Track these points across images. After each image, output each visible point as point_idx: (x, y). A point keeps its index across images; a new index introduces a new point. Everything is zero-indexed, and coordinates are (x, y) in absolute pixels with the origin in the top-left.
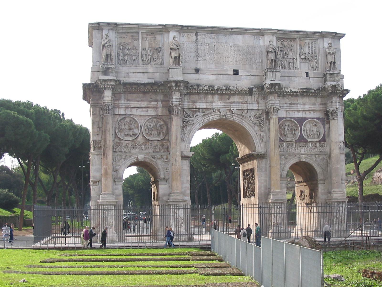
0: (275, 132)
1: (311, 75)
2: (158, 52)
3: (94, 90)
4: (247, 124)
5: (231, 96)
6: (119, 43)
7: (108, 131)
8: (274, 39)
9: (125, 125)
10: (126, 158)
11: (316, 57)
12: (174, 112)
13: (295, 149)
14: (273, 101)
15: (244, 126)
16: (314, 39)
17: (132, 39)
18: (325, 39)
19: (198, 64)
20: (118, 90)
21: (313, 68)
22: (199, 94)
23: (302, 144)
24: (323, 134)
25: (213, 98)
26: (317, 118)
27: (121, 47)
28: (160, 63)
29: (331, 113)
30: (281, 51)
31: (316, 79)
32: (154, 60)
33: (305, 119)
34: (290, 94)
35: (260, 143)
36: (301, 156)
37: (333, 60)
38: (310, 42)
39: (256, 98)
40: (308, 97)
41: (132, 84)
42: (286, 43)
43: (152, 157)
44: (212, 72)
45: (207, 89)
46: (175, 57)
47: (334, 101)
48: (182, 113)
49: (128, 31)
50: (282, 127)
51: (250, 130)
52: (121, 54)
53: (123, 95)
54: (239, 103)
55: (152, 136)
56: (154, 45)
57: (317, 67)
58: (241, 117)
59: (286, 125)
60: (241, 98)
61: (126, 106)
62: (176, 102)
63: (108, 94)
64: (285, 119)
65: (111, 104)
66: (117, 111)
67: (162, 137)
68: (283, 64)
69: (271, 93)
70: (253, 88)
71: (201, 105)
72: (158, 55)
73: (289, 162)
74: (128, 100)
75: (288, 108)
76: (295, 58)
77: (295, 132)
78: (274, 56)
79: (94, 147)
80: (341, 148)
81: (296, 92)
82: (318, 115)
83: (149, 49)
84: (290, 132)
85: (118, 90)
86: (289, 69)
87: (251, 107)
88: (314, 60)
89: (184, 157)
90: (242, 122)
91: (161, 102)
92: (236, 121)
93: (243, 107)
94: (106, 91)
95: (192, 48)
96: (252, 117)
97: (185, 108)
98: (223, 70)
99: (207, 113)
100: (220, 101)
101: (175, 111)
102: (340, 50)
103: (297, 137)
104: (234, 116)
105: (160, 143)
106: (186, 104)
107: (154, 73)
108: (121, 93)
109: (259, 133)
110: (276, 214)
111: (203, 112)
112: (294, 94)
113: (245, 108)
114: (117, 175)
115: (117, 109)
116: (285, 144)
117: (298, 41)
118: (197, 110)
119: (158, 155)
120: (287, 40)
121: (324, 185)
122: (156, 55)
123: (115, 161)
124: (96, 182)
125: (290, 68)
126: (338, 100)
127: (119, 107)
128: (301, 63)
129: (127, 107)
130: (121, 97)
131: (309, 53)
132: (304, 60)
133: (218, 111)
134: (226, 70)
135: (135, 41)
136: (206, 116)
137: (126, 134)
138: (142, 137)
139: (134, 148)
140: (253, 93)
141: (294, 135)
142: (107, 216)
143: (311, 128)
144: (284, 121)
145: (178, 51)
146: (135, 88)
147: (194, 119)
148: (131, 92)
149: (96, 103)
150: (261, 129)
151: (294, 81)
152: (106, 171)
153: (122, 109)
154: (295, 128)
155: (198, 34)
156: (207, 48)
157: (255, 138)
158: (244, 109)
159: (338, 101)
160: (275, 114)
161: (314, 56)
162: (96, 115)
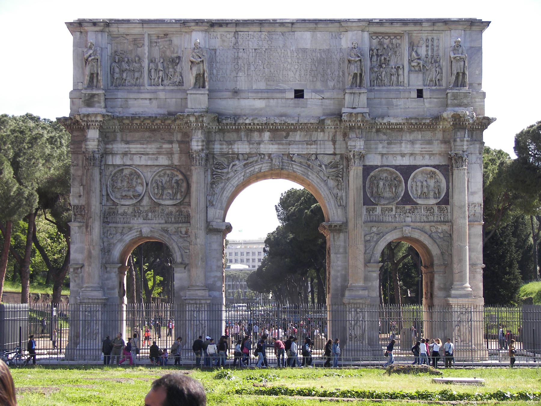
0: (355, 191)
1: (426, 94)
2: (174, 64)
3: (74, 127)
4: (315, 178)
5: (291, 133)
7: (93, 193)
8: (366, 35)
10: (124, 231)
11: (437, 65)
12: (195, 162)
13: (396, 218)
14: (353, 141)
16: (435, 32)
17: (134, 45)
18: (452, 31)
19: (238, 83)
21: (431, 81)
22: (238, 131)
24: (445, 191)
25: (260, 136)
26: (434, 166)
27: (117, 58)
28: (177, 83)
29: (455, 160)
30: (377, 55)
31: (435, 100)
32: (169, 77)
33: (415, 167)
34: (388, 127)
35: (336, 208)
36: (404, 228)
37: (460, 70)
38: (430, 38)
40: (421, 131)
41: (133, 118)
42: (387, 42)
45: (250, 124)
47: (458, 140)
50: (375, 182)
52: (117, 70)
53: (119, 136)
55: (164, 197)
56: (168, 53)
57: (439, 80)
59: (380, 179)
61: (124, 152)
62: (198, 146)
63: (93, 134)
66: (110, 160)
67: (180, 199)
69: (351, 128)
70: (324, 120)
71: (242, 148)
72: (175, 70)
73: (385, 239)
74: (127, 143)
76: (401, 67)
77: (396, 189)
80: (477, 215)
81: (398, 125)
82: (437, 161)
84: (388, 189)
85: (111, 127)
86: (390, 86)
87: (323, 150)
88: (434, 69)
90: (307, 174)
91: (177, 145)
93: (309, 150)
94: (90, 130)
96: (323, 166)
97: (215, 153)
100: (272, 141)
101: (196, 161)
102: (479, 50)
103: (398, 198)
104: (294, 164)
105: (175, 209)
106: (217, 148)
107: (167, 100)
108: (116, 131)
109: (335, 191)
110: (353, 322)
111: (245, 160)
112: (396, 127)
113: (313, 151)
114: (110, 258)
115: (111, 156)
116: (379, 209)
117: (406, 39)
118: (235, 157)
119: (172, 228)
120: (389, 37)
126: (466, 135)
127: (113, 154)
129: (125, 154)
130: (115, 137)
131: (427, 57)
134: (283, 91)
135: (139, 49)
136: (249, 165)
137: (124, 194)
139: (135, 216)
140: (326, 127)
142: (91, 320)
143: (425, 183)
144: (379, 171)
145: (201, 65)
149: (78, 148)
150: (338, 185)
151: (397, 106)
152: (90, 252)
155: (238, 34)
156: (253, 57)
158: (312, 153)
160: (356, 162)
161: (436, 61)
162: (78, 165)
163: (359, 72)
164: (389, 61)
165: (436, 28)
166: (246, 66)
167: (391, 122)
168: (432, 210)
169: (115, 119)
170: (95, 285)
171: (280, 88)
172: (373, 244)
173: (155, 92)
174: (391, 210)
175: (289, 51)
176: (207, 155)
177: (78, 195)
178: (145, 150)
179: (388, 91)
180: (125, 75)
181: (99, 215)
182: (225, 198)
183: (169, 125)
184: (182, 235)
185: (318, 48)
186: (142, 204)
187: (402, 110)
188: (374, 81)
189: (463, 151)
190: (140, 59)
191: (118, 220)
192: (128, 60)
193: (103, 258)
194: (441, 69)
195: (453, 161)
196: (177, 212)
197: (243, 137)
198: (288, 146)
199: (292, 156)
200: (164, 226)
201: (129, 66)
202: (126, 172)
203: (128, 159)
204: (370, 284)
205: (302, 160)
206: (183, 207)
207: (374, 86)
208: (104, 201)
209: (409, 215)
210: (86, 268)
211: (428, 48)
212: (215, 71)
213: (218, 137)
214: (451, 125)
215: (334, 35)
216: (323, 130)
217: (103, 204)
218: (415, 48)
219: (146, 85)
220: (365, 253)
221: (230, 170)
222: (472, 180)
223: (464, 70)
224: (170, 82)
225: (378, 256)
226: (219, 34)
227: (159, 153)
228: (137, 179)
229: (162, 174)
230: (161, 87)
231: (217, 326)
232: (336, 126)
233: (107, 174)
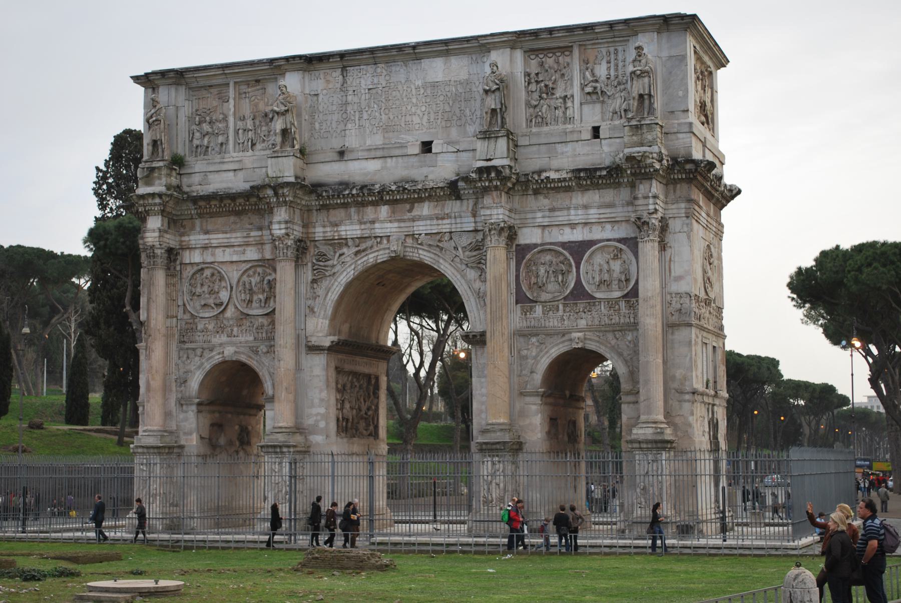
2: (268, 120)
5: (416, 205)
6: (194, 110)
8: (519, 55)
9: (202, 285)
11: (622, 87)
13: (564, 320)
14: (488, 208)
19: (347, 139)
22: (345, 206)
23: (582, 306)
24: (635, 278)
25: (376, 211)
26: (619, 241)
30: (537, 82)
33: (590, 243)
34: (549, 186)
35: (478, 309)
38: (612, 49)
39: (471, 202)
40: (598, 189)
41: (209, 198)
44: (373, 154)
47: (640, 196)
49: (209, 83)
51: (455, 279)
53: (198, 222)
54: (431, 219)
55: (254, 304)
56: (262, 107)
58: (437, 251)
60: (436, 206)
62: (280, 229)
64: (539, 248)
65: (160, 245)
68: (540, 113)
69: (486, 190)
70: (456, 181)
71: (350, 230)
73: (547, 352)
74: (207, 232)
75: (546, 222)
80: (683, 311)
84: (553, 279)
87: (459, 226)
89: (313, 349)
92: (426, 262)
93: (440, 227)
97: (316, 239)
98: (398, 145)
99: (365, 247)
104: (420, 249)
106: (319, 232)
109: (477, 285)
115: (188, 251)
116: (539, 309)
117: (576, 52)
120: (554, 53)
122: (264, 128)
125: (556, 120)
129: (205, 248)
132: (594, 97)
133: (388, 241)
138: (233, 310)
140: (462, 192)
141: (564, 284)
144: (539, 252)
146: (215, 205)
148: (212, 215)
151: (562, 153)
153: (197, 252)
157: (466, 297)
158: (444, 231)
163: (499, 106)
164: (553, 89)
166: (357, 113)
167: (551, 177)
168: (617, 307)
170: (155, 428)
172: (530, 361)
175: (413, 87)
178: (229, 241)
182: (330, 302)
183: (256, 204)
185: (453, 79)
187: (570, 159)
188: (531, 121)
189: (649, 213)
190: (225, 119)
191: (197, 338)
197: (353, 214)
199: (417, 236)
200: (250, 345)
201: (212, 128)
207: (531, 127)
212: (317, 126)
213: (322, 217)
215: (474, 59)
216: (458, 197)
219: (231, 152)
222: (676, 259)
223: (650, 92)
225: (538, 377)
227: (247, 244)
228: (220, 280)
231: (319, 484)
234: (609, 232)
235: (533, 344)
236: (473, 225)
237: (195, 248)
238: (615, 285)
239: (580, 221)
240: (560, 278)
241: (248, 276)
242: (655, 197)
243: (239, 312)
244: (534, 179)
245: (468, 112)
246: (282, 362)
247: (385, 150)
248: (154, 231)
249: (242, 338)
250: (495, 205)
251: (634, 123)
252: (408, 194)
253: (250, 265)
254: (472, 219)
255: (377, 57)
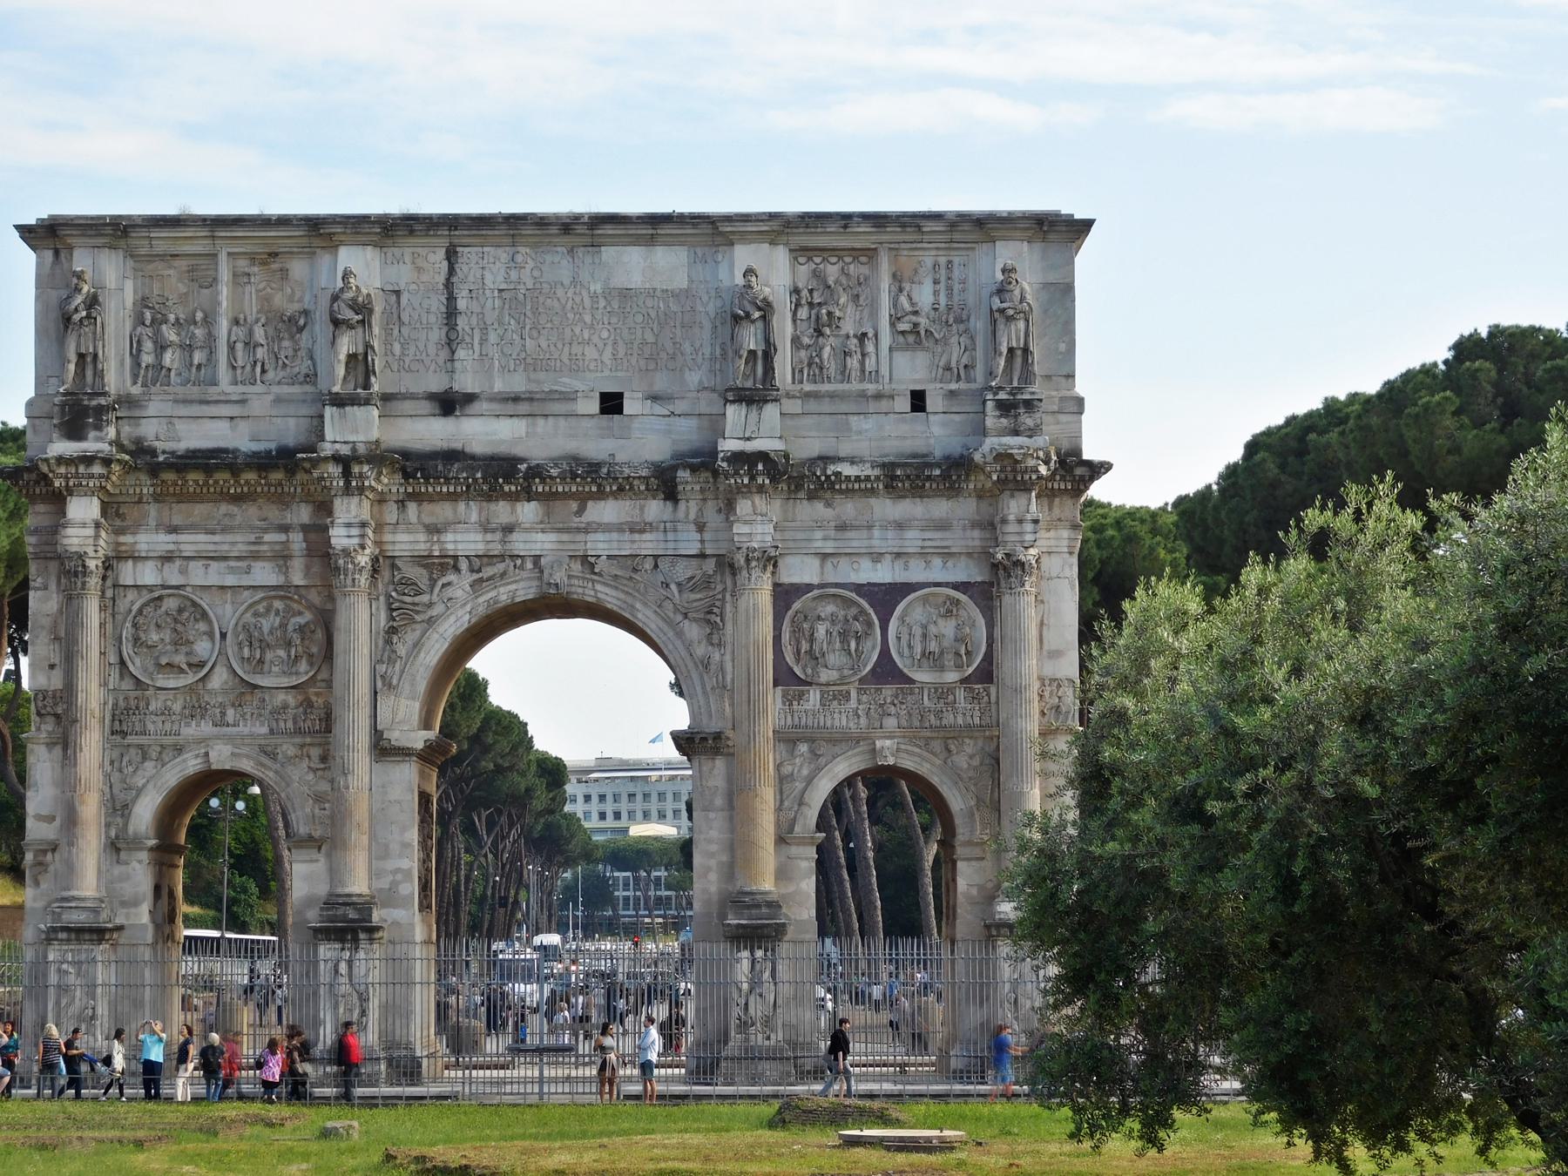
3: (38, 491)
4: (653, 616)
5: (590, 504)
8: (781, 255)
9: (158, 626)
11: (962, 327)
13: (859, 717)
14: (746, 522)
15: (640, 625)
16: (956, 245)
19: (456, 376)
20: (131, 491)
21: (948, 368)
23: (889, 692)
25: (513, 511)
26: (956, 586)
27: (148, 315)
28: (302, 379)
29: (1005, 568)
30: (811, 305)
31: (957, 418)
32: (280, 362)
33: (907, 589)
34: (837, 487)
35: (705, 692)
37: (1018, 339)
38: (943, 260)
42: (832, 271)
43: (265, 753)
46: (352, 358)
47: (1012, 517)
48: (386, 574)
52: (148, 345)
55: (266, 667)
56: (278, 300)
59: (819, 618)
61: (164, 554)
63: (83, 509)
64: (816, 592)
66: (128, 573)
67: (307, 673)
68: (817, 360)
70: (674, 468)
72: (296, 343)
74: (173, 530)
75: (829, 547)
76: (870, 335)
77: (858, 644)
78: (760, 336)
79: (39, 714)
80: (1064, 709)
83: (257, 321)
84: (838, 645)
85: (131, 491)
87: (671, 545)
88: (954, 340)
90: (633, 606)
91: (301, 535)
92: (609, 606)
93: (635, 546)
95: (433, 309)
96: (673, 587)
98: (557, 396)
100: (541, 522)
103: (865, 666)
111: (472, 571)
114: (126, 825)
115: (130, 563)
116: (814, 696)
120: (840, 258)
121: (983, 863)
122: (286, 343)
123: (120, 771)
124: (45, 852)
126: (1033, 507)
128: (895, 354)
129: (167, 558)
131: (936, 309)
132: (911, 339)
137: (163, 662)
138: (225, 676)
140: (680, 488)
143: (933, 629)
144: (814, 599)
146: (197, 482)
147: (435, 598)
148: (184, 498)
151: (860, 433)
153: (150, 564)
154: (858, 626)
159: (1029, 517)
162: (46, 588)
163: (761, 347)
165: (957, 236)
166: (477, 331)
168: (951, 698)
169: (140, 469)
171: (563, 389)
173: (243, 402)
174: (847, 696)
175: (585, 293)
176: (375, 560)
177: (47, 663)
179: (832, 396)
180: (168, 358)
181: (97, 714)
182: (421, 669)
183: (280, 484)
184: (312, 765)
186: (210, 686)
188: (801, 371)
190: (209, 321)
192: (177, 319)
193: (108, 825)
194: (972, 338)
195: (1001, 572)
196: (301, 704)
198: (580, 537)
199: (592, 560)
200: (263, 742)
202: (171, 604)
203: (176, 571)
204: (791, 888)
205: (619, 573)
206: (317, 694)
208: (111, 679)
209: (892, 710)
210: (63, 848)
211: (938, 287)
212: (397, 348)
214: (994, 483)
217: (111, 687)
218: (907, 286)
220: (779, 809)
221: (435, 598)
224: (282, 374)
225: (812, 815)
226: (408, 251)
227: (256, 556)
228: (196, 620)
229: (261, 608)
230: (259, 388)
232: (703, 485)
233: (122, 610)
234: (937, 572)
235: (802, 755)
236: (699, 545)
237: (146, 558)
238: (949, 660)
239: (889, 550)
240: (853, 645)
241: (256, 614)
242: (1036, 522)
243: (237, 680)
244: (815, 474)
245: (687, 347)
246: (350, 777)
247: (535, 404)
248: (84, 525)
249: (243, 729)
250: (759, 518)
251: (1002, 396)
252: (578, 485)
253: (261, 595)
254: (698, 536)
255: (520, 235)
